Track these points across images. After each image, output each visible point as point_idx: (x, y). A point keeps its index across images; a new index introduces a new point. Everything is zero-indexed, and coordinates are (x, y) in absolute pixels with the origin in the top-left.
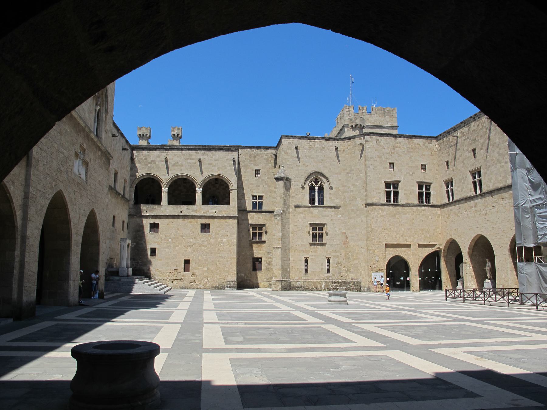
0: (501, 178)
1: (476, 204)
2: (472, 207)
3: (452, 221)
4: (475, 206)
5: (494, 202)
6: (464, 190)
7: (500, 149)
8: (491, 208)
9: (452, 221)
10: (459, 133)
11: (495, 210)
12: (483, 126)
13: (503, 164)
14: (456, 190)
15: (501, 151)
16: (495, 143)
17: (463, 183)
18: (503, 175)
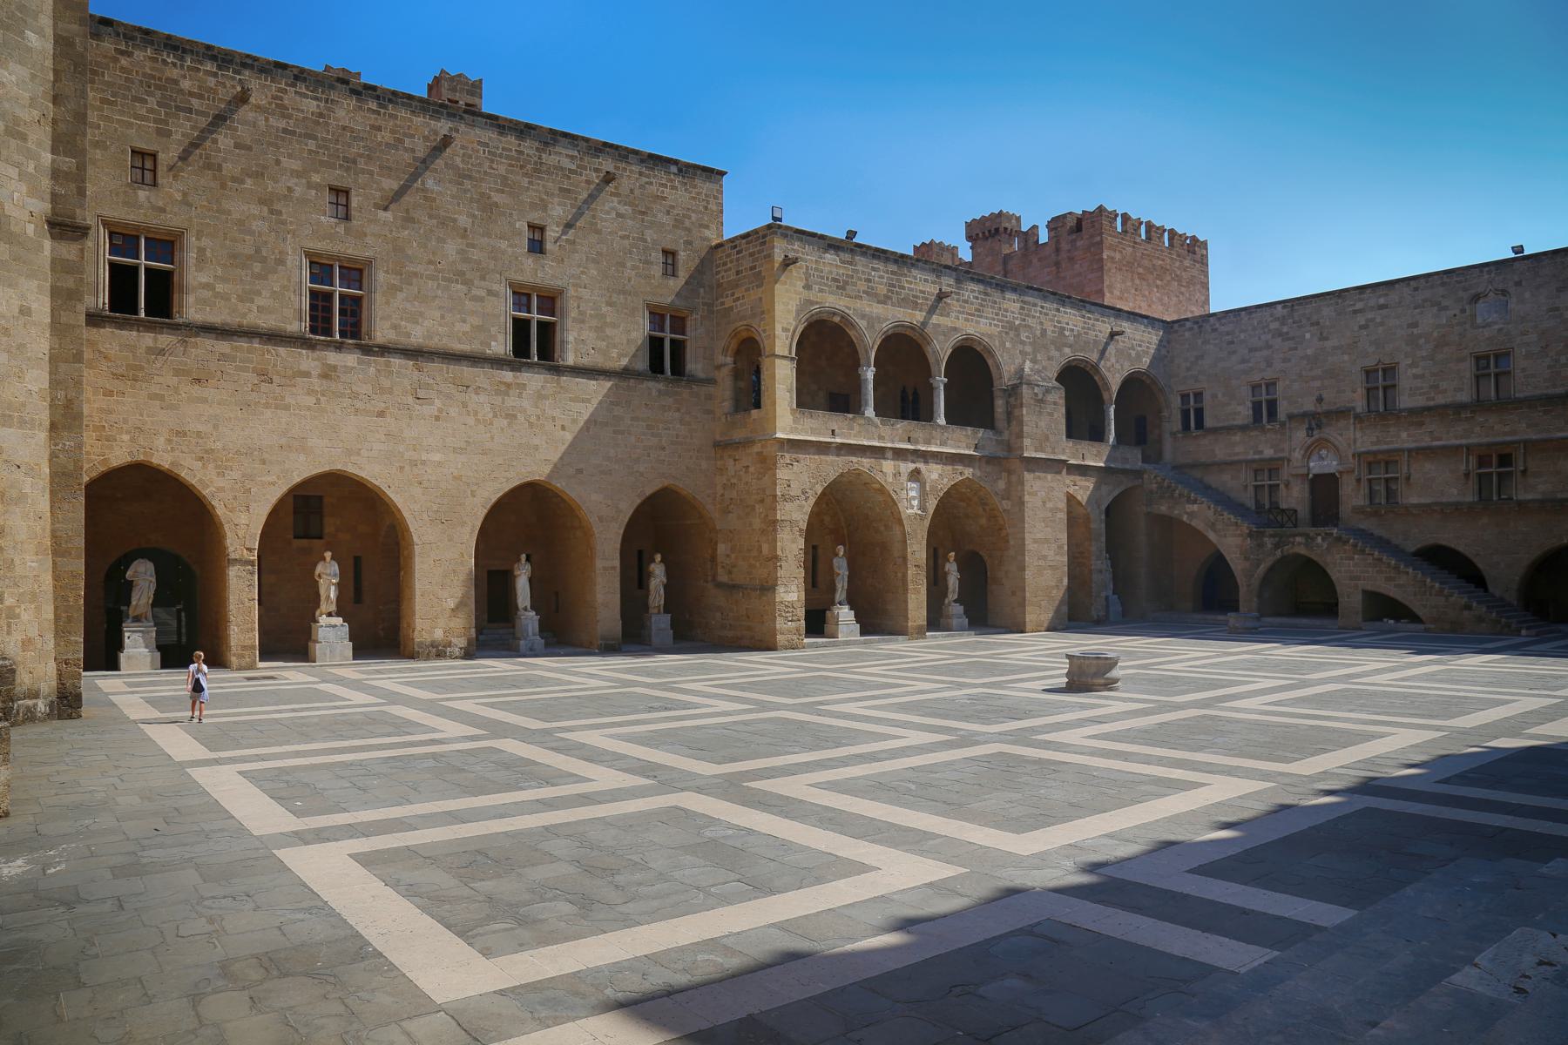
0: (467, 328)
1: (334, 368)
2: (307, 374)
3: (162, 398)
4: (325, 376)
5: (428, 387)
6: (260, 301)
7: (473, 246)
8: (410, 400)
9: (162, 398)
10: (261, 91)
11: (428, 410)
12: (401, 141)
13: (475, 292)
14: (207, 286)
15: (475, 254)
16: (455, 220)
17: (261, 277)
18: (476, 321)
